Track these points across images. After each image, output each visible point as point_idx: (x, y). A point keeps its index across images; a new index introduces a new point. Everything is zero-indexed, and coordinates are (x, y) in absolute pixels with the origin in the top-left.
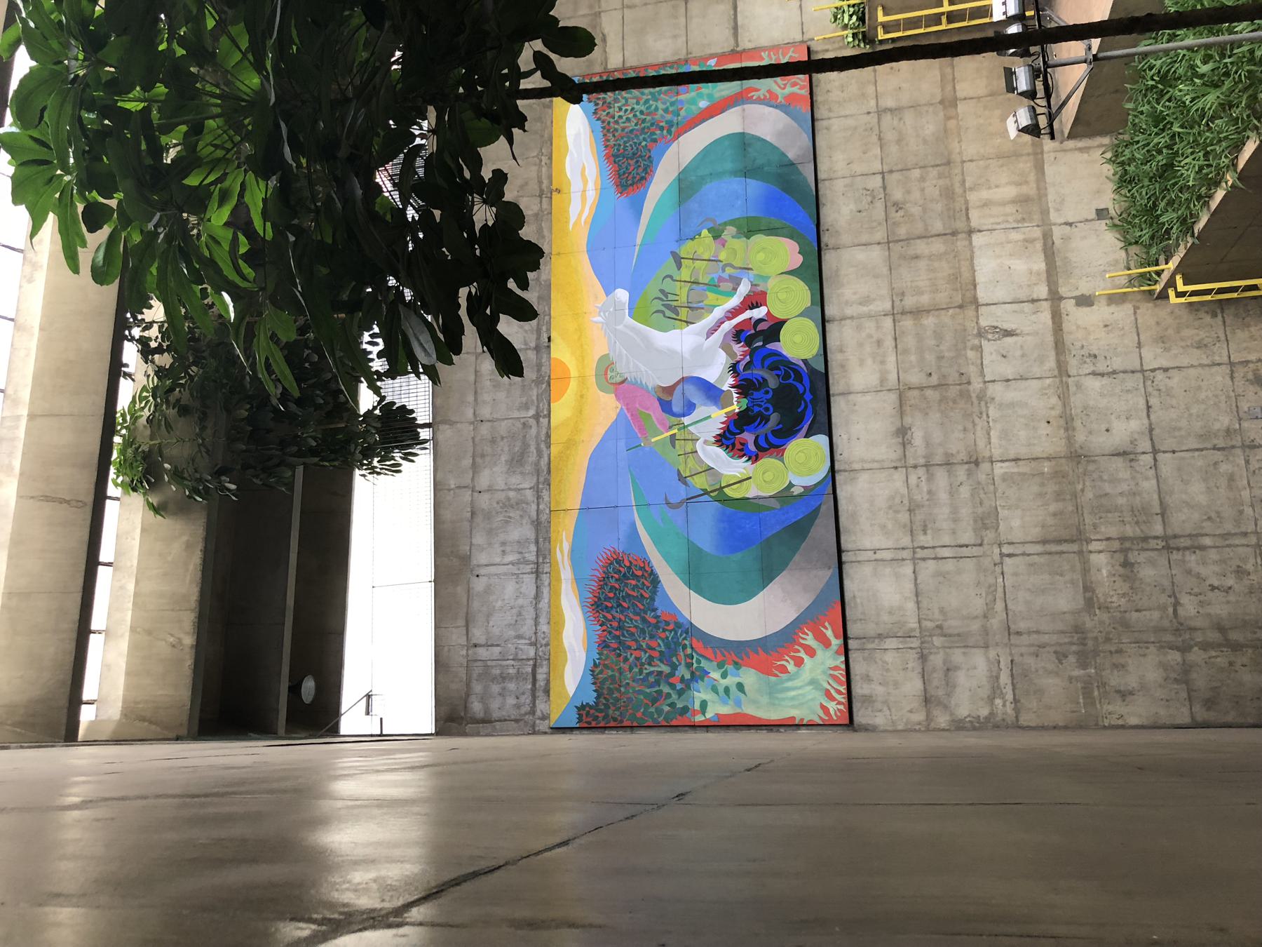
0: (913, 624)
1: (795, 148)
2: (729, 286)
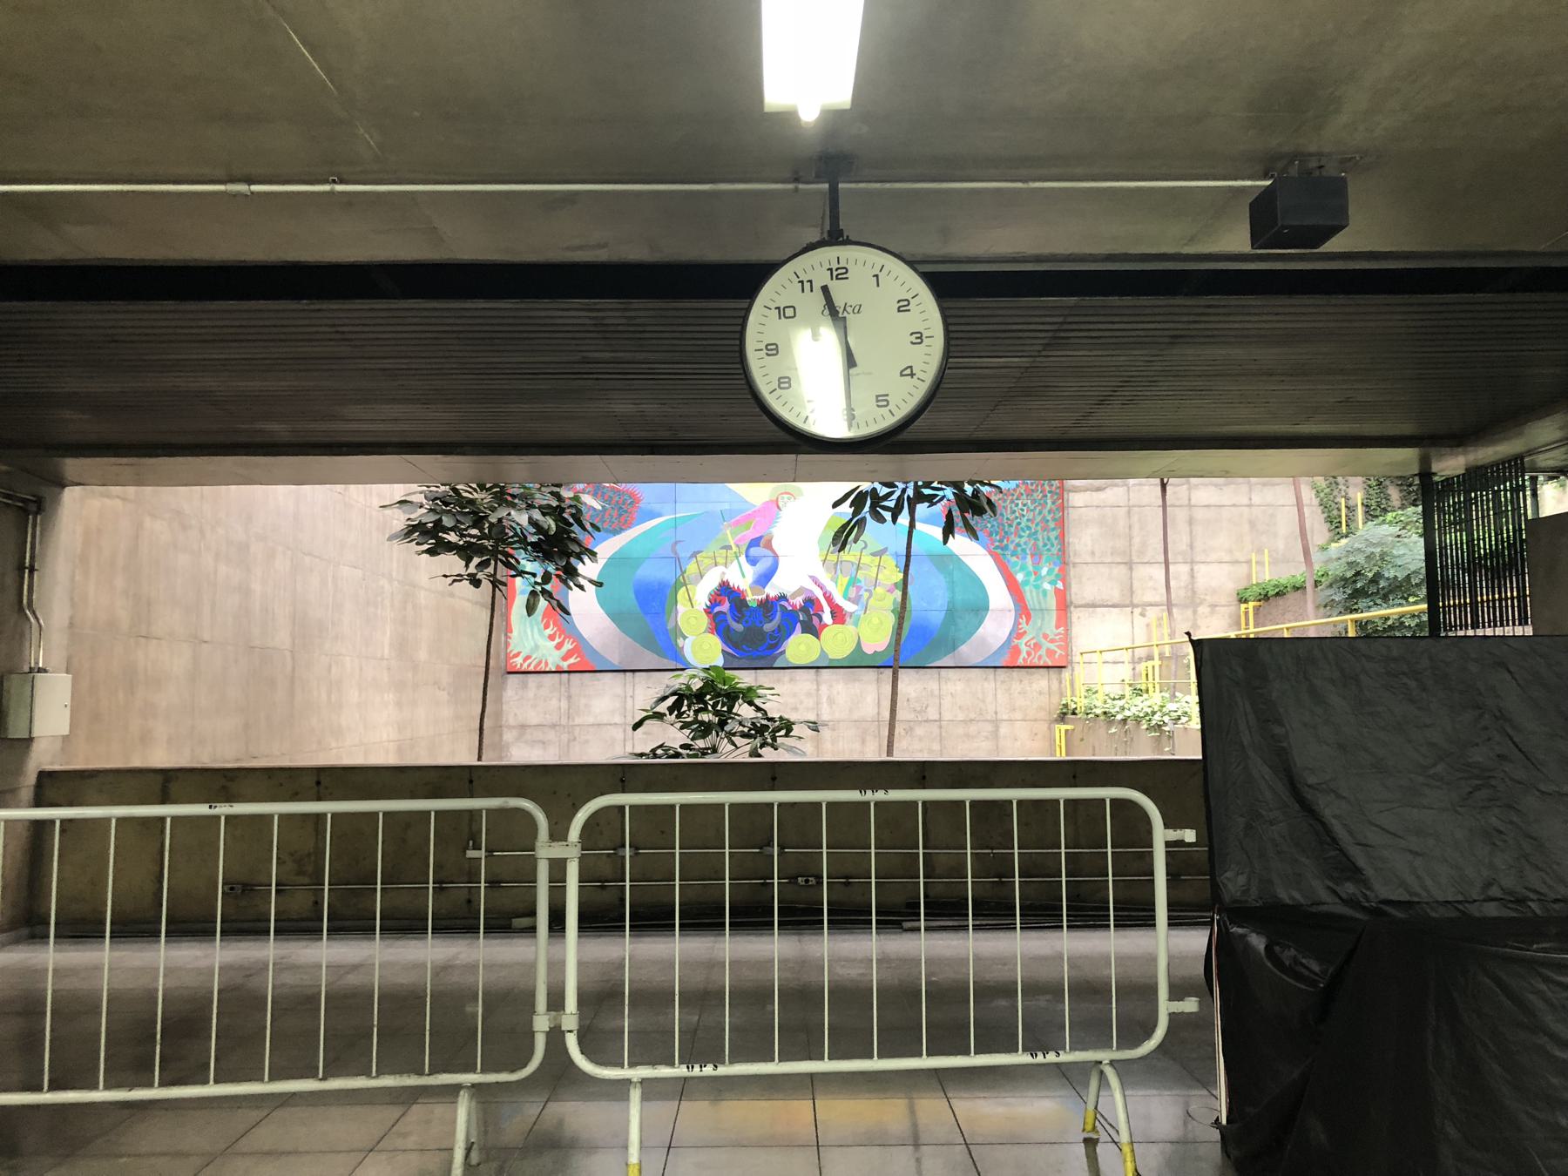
0: (577, 721)
1: (967, 652)
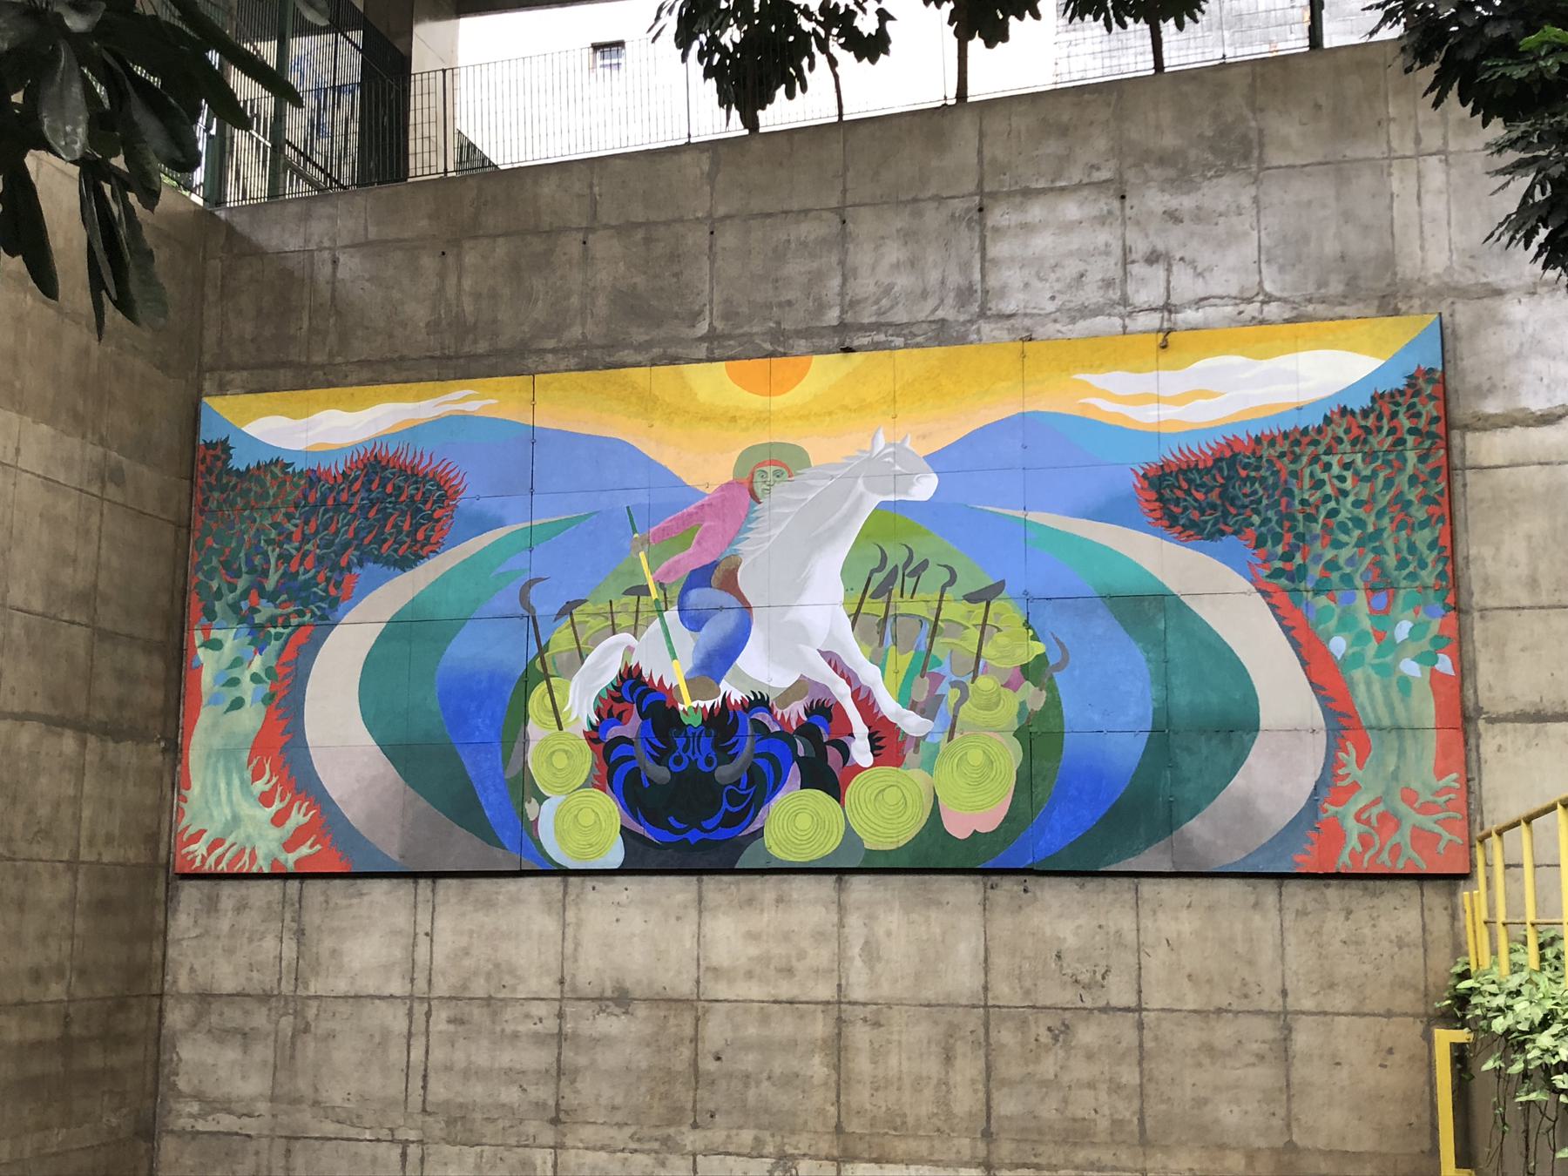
0: (315, 987)
2: (921, 696)
